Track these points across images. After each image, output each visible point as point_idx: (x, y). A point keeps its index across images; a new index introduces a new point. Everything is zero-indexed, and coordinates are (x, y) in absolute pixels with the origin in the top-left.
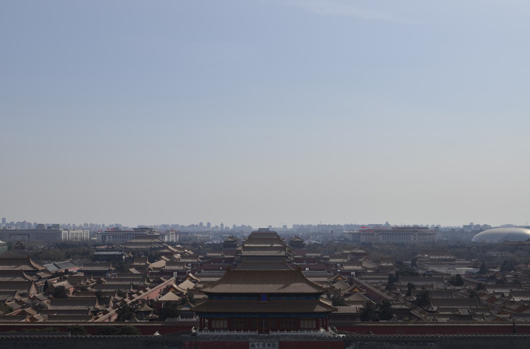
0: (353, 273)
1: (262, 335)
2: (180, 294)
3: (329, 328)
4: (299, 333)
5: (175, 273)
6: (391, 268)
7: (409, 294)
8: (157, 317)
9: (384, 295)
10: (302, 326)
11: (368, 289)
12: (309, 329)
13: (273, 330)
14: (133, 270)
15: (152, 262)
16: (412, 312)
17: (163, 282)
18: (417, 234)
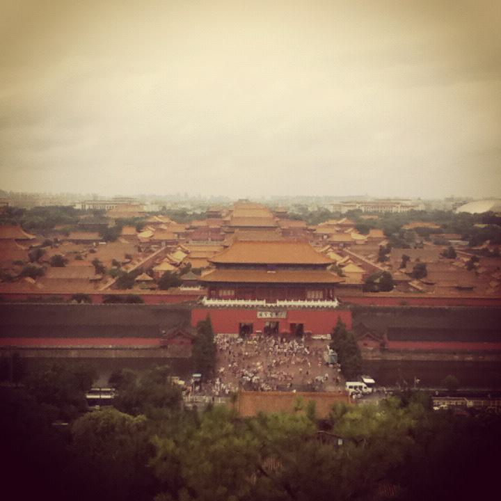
0: (342, 245)
1: (269, 305)
2: (175, 265)
3: (336, 300)
4: (306, 303)
5: (163, 244)
6: (379, 240)
7: (403, 266)
8: (157, 286)
9: (378, 266)
10: (309, 297)
11: (361, 261)
12: (315, 300)
13: (280, 300)
14: (123, 241)
15: (139, 231)
16: (410, 283)
17: (153, 252)
18: (399, 206)
